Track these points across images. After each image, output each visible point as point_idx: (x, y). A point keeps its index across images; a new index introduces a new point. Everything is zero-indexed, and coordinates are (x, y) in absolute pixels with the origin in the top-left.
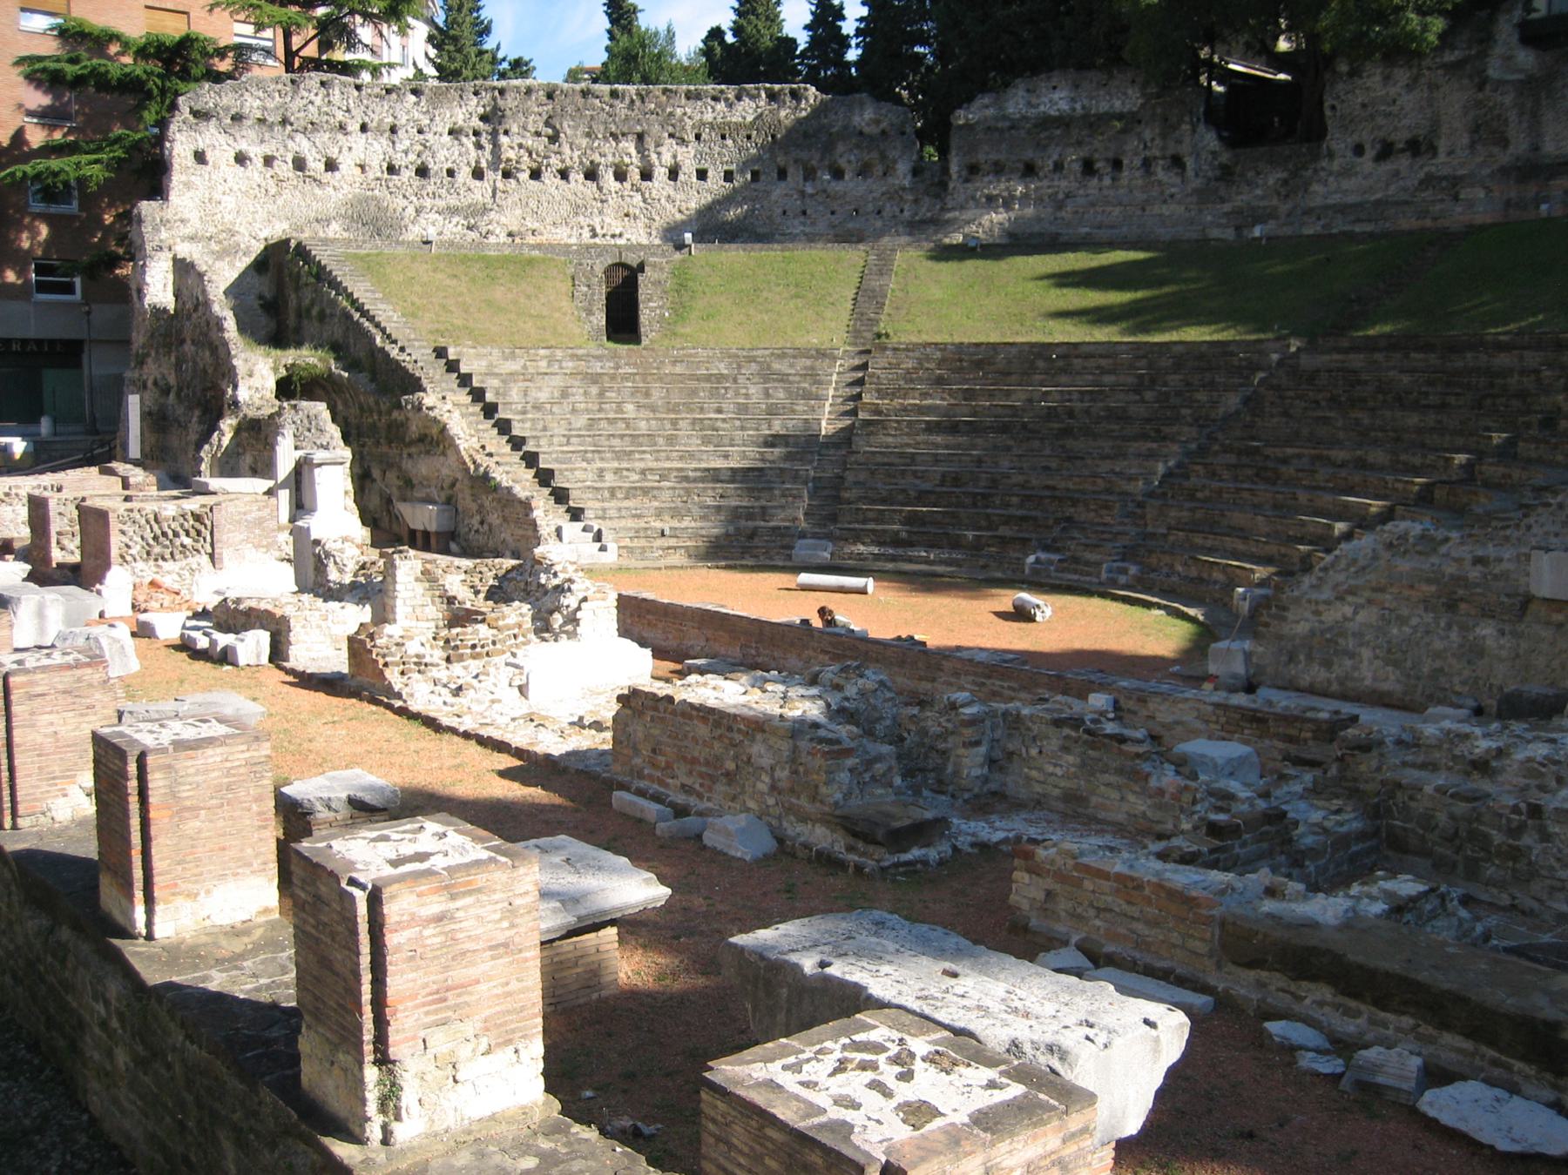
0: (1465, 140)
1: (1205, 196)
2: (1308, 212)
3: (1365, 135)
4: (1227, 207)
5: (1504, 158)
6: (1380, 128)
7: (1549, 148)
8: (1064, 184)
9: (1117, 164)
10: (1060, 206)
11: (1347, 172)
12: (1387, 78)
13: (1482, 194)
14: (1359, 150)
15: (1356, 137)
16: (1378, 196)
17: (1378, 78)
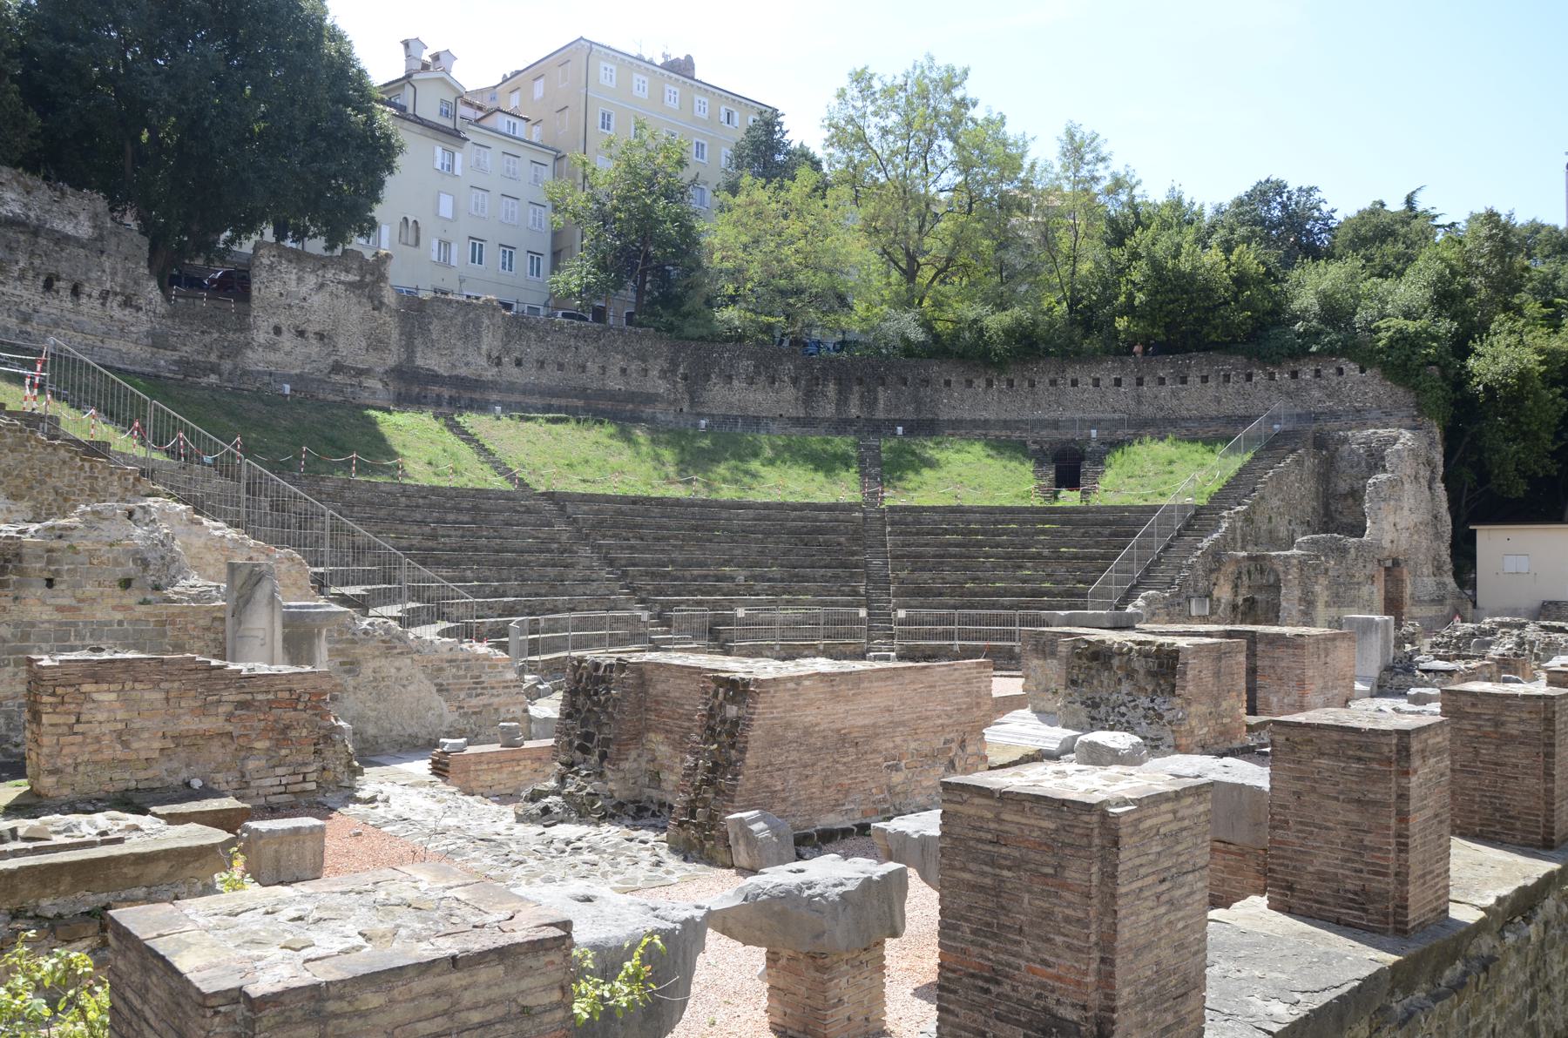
0: (364, 344)
1: (158, 341)
2: (245, 373)
3: (282, 320)
4: (176, 356)
5: (392, 361)
6: (295, 317)
7: (419, 362)
8: (25, 294)
9: (76, 291)
10: (26, 319)
11: (272, 347)
12: (300, 280)
13: (380, 386)
14: (278, 331)
15: (274, 321)
16: (298, 371)
17: (294, 277)
